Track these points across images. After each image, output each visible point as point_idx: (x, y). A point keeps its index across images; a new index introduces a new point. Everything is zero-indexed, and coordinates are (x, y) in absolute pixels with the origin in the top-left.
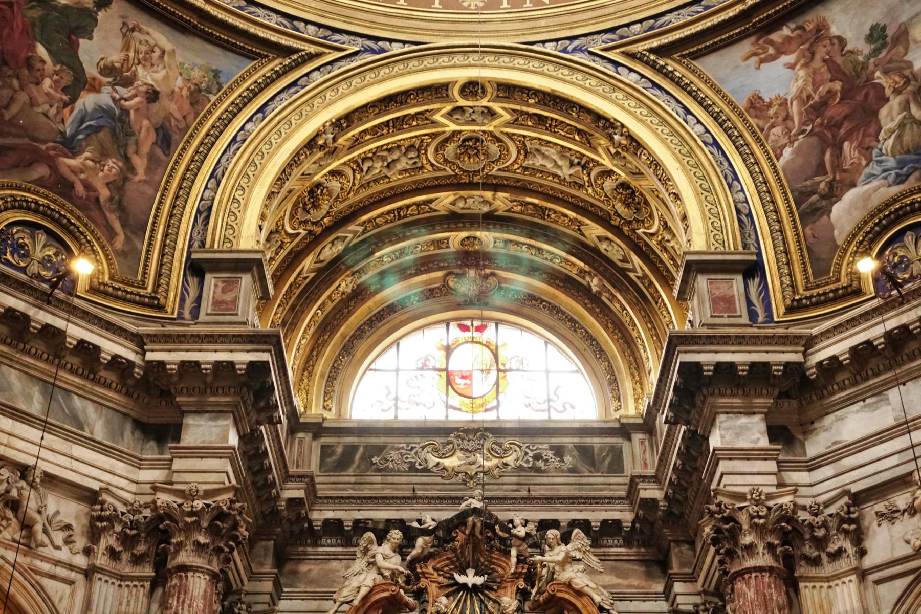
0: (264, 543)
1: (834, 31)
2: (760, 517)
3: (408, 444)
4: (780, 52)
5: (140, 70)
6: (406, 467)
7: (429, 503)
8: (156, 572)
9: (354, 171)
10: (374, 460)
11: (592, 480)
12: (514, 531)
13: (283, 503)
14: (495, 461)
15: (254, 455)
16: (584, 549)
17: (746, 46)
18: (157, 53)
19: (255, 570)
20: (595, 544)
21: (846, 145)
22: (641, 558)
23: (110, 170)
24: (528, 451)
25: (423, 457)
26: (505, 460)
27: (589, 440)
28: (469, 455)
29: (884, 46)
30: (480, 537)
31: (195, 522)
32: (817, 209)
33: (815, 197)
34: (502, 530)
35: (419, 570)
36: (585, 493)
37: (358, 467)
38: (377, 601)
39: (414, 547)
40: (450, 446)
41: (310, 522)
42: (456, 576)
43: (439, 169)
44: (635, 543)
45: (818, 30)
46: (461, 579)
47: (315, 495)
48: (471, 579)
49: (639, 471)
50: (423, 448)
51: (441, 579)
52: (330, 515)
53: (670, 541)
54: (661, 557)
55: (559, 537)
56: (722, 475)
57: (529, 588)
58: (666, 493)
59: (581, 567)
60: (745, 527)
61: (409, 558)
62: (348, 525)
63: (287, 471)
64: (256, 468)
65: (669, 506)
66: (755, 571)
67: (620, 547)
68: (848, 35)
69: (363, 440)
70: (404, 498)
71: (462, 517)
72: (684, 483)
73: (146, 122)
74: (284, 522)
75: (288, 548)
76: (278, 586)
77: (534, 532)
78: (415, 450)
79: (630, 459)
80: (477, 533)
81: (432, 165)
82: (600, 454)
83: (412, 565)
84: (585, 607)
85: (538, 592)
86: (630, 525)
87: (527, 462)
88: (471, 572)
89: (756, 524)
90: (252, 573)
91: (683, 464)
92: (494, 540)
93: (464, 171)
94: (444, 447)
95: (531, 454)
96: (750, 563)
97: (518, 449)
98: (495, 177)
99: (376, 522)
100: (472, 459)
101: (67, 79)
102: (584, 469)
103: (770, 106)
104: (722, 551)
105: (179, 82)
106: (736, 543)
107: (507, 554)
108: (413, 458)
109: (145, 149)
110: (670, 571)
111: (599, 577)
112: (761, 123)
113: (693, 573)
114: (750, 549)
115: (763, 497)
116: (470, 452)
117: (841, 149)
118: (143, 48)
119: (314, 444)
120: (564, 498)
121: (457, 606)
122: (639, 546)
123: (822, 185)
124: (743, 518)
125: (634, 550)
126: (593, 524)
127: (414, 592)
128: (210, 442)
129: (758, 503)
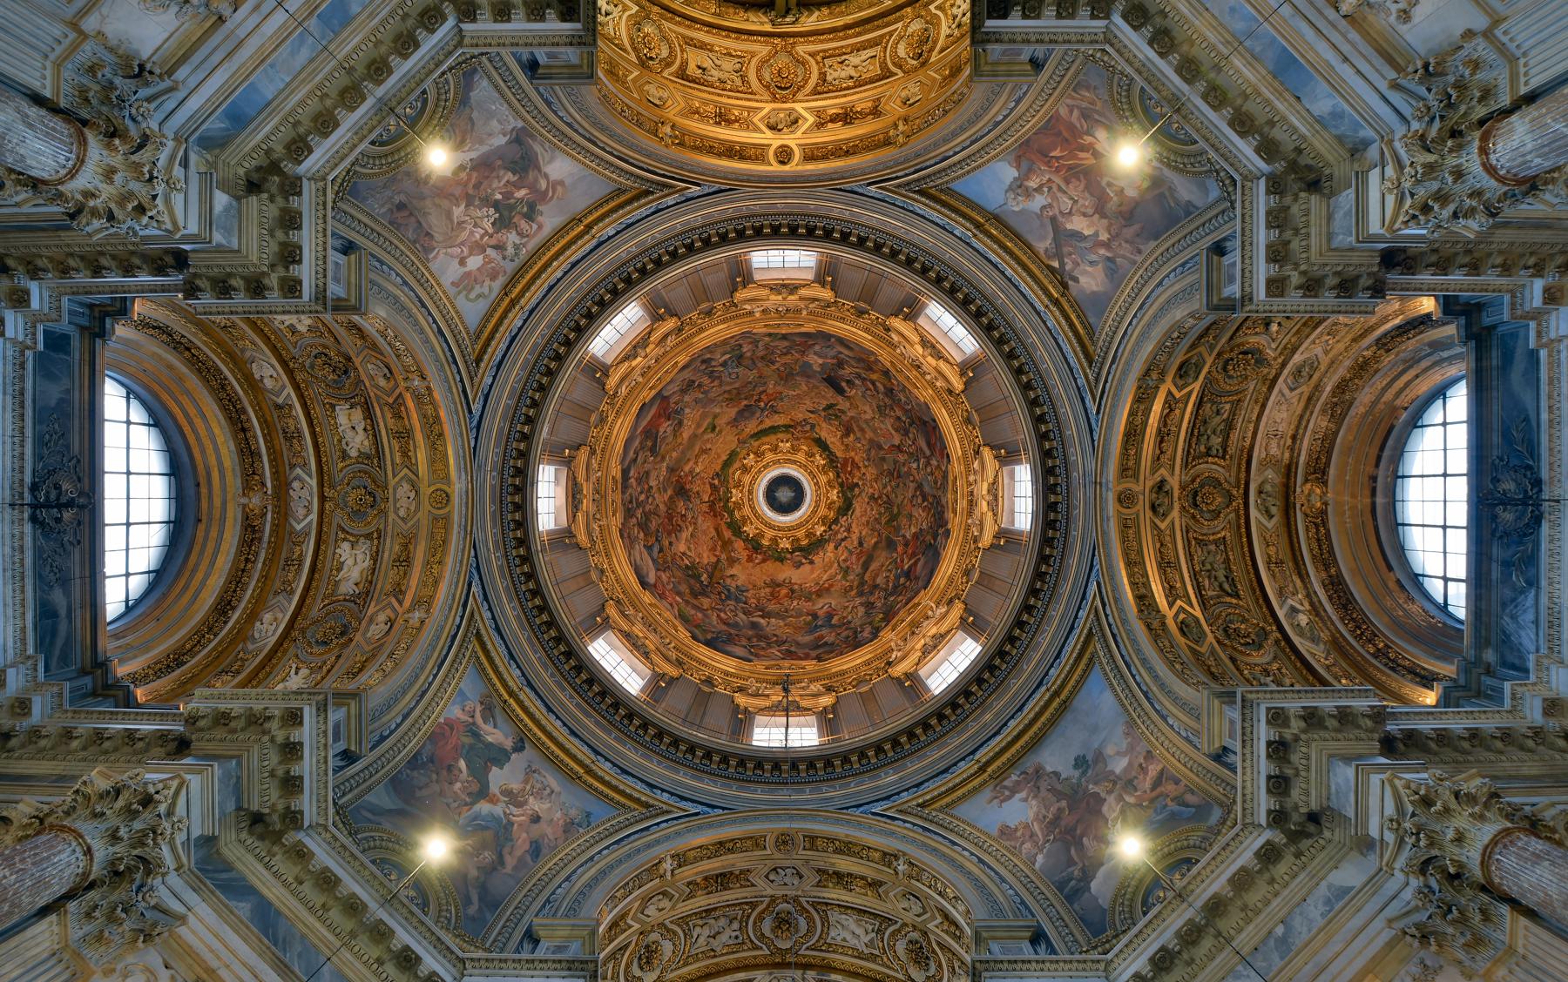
1: (1049, 769)
4: (1013, 791)
5: (531, 799)
9: (685, 935)
17: (987, 793)
18: (548, 791)
21: (1085, 840)
23: (485, 858)
29: (1088, 767)
32: (1078, 890)
33: (1073, 883)
43: (758, 948)
45: (1037, 772)
68: (1059, 769)
73: (524, 835)
81: (751, 941)
93: (778, 949)
98: (804, 956)
101: (475, 787)
103: (1016, 830)
105: (559, 815)
109: (518, 853)
112: (1013, 843)
117: (1082, 845)
118: (538, 786)
123: (1076, 873)
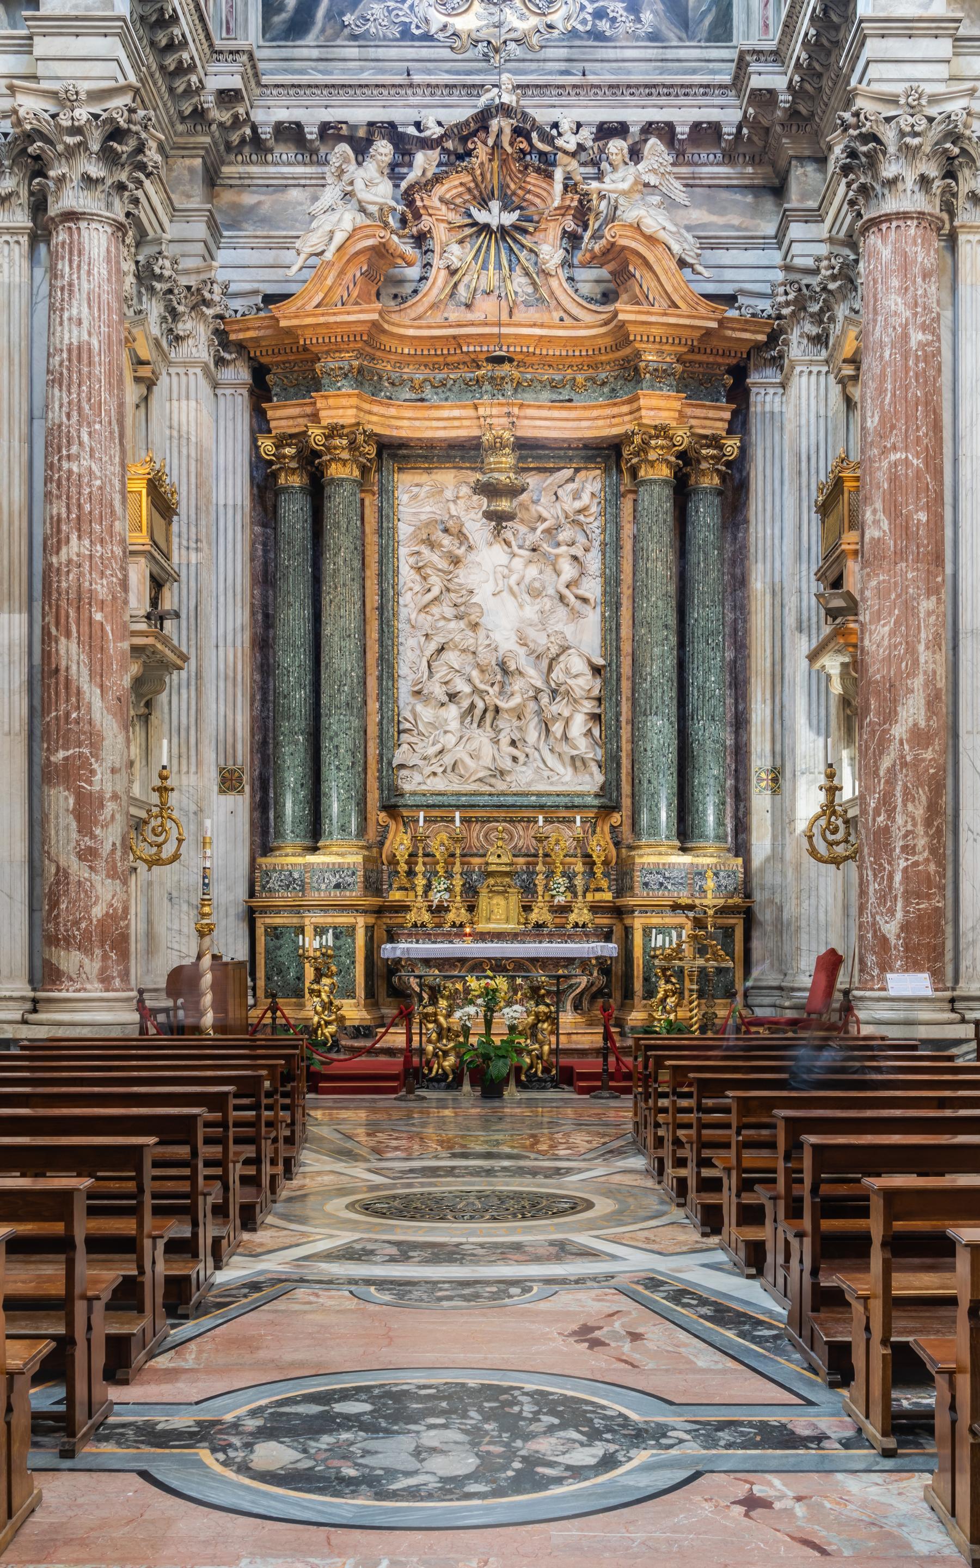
2: (916, 134)
6: (396, 31)
7: (432, 95)
8: (34, 220)
10: (348, 18)
11: (682, 53)
12: (559, 142)
13: (211, 98)
14: (534, 21)
15: (157, 21)
19: (177, 206)
22: (747, 182)
25: (420, 14)
26: (549, 19)
31: (79, 144)
34: (542, 141)
35: (419, 203)
36: (668, 79)
37: (323, 31)
38: (358, 253)
39: (410, 165)
41: (254, 128)
42: (474, 212)
44: (741, 160)
46: (481, 217)
47: (258, 84)
48: (495, 216)
49: (754, 42)
51: (451, 216)
52: (283, 115)
53: (792, 157)
54: (776, 181)
55: (626, 151)
56: (868, 63)
57: (580, 230)
58: (791, 81)
59: (656, 199)
60: (892, 149)
61: (404, 185)
62: (311, 133)
63: (211, 46)
64: (164, 43)
65: (794, 102)
66: (897, 219)
67: (718, 164)
71: (482, 120)
72: (817, 66)
74: (214, 127)
75: (226, 170)
76: (214, 227)
77: (589, 143)
79: (744, 16)
82: (697, 8)
83: (408, 198)
85: (593, 237)
86: (734, 130)
87: (584, 22)
88: (495, 205)
89: (907, 146)
91: (818, 35)
92: (530, 153)
95: (590, 8)
96: (890, 205)
99: (354, 128)
102: (672, 35)
104: (854, 186)
106: (875, 176)
107: (549, 176)
110: (786, 206)
111: (682, 212)
114: (892, 183)
115: (924, 102)
120: (637, 86)
122: (745, 164)
124: (889, 135)
125: (738, 169)
126: (678, 129)
127: (412, 237)
128: (87, 8)
129: (913, 110)
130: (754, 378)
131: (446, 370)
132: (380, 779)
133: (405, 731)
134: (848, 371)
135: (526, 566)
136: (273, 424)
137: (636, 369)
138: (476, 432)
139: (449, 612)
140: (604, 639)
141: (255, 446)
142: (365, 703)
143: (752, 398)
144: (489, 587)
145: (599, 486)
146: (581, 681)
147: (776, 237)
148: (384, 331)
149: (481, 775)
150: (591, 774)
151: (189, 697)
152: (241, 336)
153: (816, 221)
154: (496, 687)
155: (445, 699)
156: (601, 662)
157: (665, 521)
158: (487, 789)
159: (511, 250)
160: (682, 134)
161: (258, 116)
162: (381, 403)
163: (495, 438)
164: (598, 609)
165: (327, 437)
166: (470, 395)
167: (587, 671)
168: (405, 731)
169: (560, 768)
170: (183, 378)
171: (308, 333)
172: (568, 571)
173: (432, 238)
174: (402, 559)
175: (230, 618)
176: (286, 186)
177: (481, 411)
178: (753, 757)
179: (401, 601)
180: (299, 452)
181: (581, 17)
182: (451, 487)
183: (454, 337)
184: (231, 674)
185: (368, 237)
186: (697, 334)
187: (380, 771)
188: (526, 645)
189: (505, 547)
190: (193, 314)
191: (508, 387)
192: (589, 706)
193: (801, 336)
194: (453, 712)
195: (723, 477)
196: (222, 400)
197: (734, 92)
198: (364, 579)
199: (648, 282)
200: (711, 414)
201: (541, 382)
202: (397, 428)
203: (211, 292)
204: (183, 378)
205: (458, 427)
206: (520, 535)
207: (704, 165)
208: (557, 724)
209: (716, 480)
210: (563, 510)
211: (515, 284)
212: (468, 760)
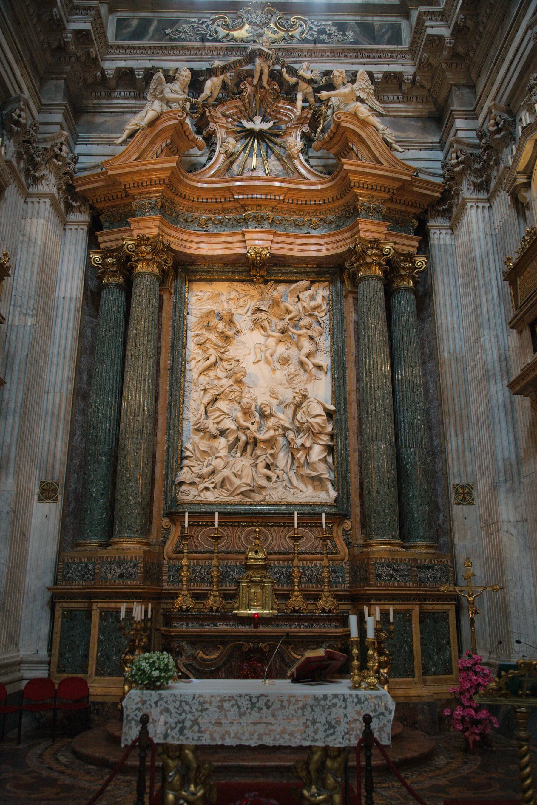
0: (54, 82)
3: (199, 19)
16: (368, 91)
20: (377, 95)
24: (313, 27)
25: (213, 29)
27: (369, 19)
28: (256, 28)
30: (267, 87)
40: (240, 20)
41: (103, 71)
44: (414, 99)
46: (248, 125)
50: (214, 21)
51: (229, 126)
52: (122, 64)
53: (452, 85)
62: (140, 75)
65: (455, 44)
67: (400, 102)
69: (156, 14)
70: (193, 48)
74: (73, 59)
75: (84, 101)
78: (206, 24)
80: (265, 84)
84: (369, 137)
86: (411, 77)
87: (312, 35)
88: (258, 119)
90: (42, 104)
94: (233, 21)
97: (303, 24)
100: (261, 31)
107: (292, 101)
108: (204, 30)
110: (453, 108)
113: (475, 109)
116: (258, 26)
119: (110, 17)
121: (244, 150)
125: (412, 106)
126: (376, 76)
130: (431, 223)
131: (223, 215)
132: (165, 493)
133: (187, 458)
134: (522, 179)
135: (277, 344)
136: (102, 246)
137: (355, 208)
138: (243, 251)
139: (221, 374)
140: (334, 393)
141: (88, 259)
142: (156, 435)
143: (432, 235)
144: (252, 358)
145: (328, 292)
146: (318, 420)
147: (439, 143)
148: (181, 182)
149: (243, 489)
150: (327, 491)
151: (14, 421)
152: (84, 188)
153: (473, 119)
154: (256, 426)
155: (216, 432)
156: (332, 408)
157: (380, 304)
158: (247, 500)
159: (268, 146)
160: (378, 78)
161: (107, 64)
162: (177, 230)
163: (256, 253)
164: (329, 374)
165: (136, 246)
166: (239, 228)
167: (324, 414)
168: (187, 458)
169: (302, 486)
170: (36, 205)
171: (127, 180)
172: (307, 346)
173: (216, 136)
174: (189, 339)
175: (60, 373)
176: (123, 113)
177: (247, 236)
178: (451, 476)
179: (187, 367)
180: (118, 260)
181: (310, 33)
182: (225, 294)
183: (229, 189)
184: (56, 412)
185: (171, 119)
186: (397, 185)
187: (166, 486)
188: (277, 398)
189: (262, 331)
190: (47, 165)
191: (266, 222)
192: (325, 439)
193: (469, 185)
194: (222, 442)
195: (416, 283)
196: (68, 232)
197: (410, 56)
198: (159, 348)
199: (362, 152)
200: (406, 242)
201: (288, 221)
202: (188, 248)
203: (61, 150)
204: (36, 205)
205: (231, 248)
206: (273, 324)
207: (391, 103)
208: (301, 453)
209: (411, 284)
210: (304, 307)
211: (270, 165)
212: (233, 478)
